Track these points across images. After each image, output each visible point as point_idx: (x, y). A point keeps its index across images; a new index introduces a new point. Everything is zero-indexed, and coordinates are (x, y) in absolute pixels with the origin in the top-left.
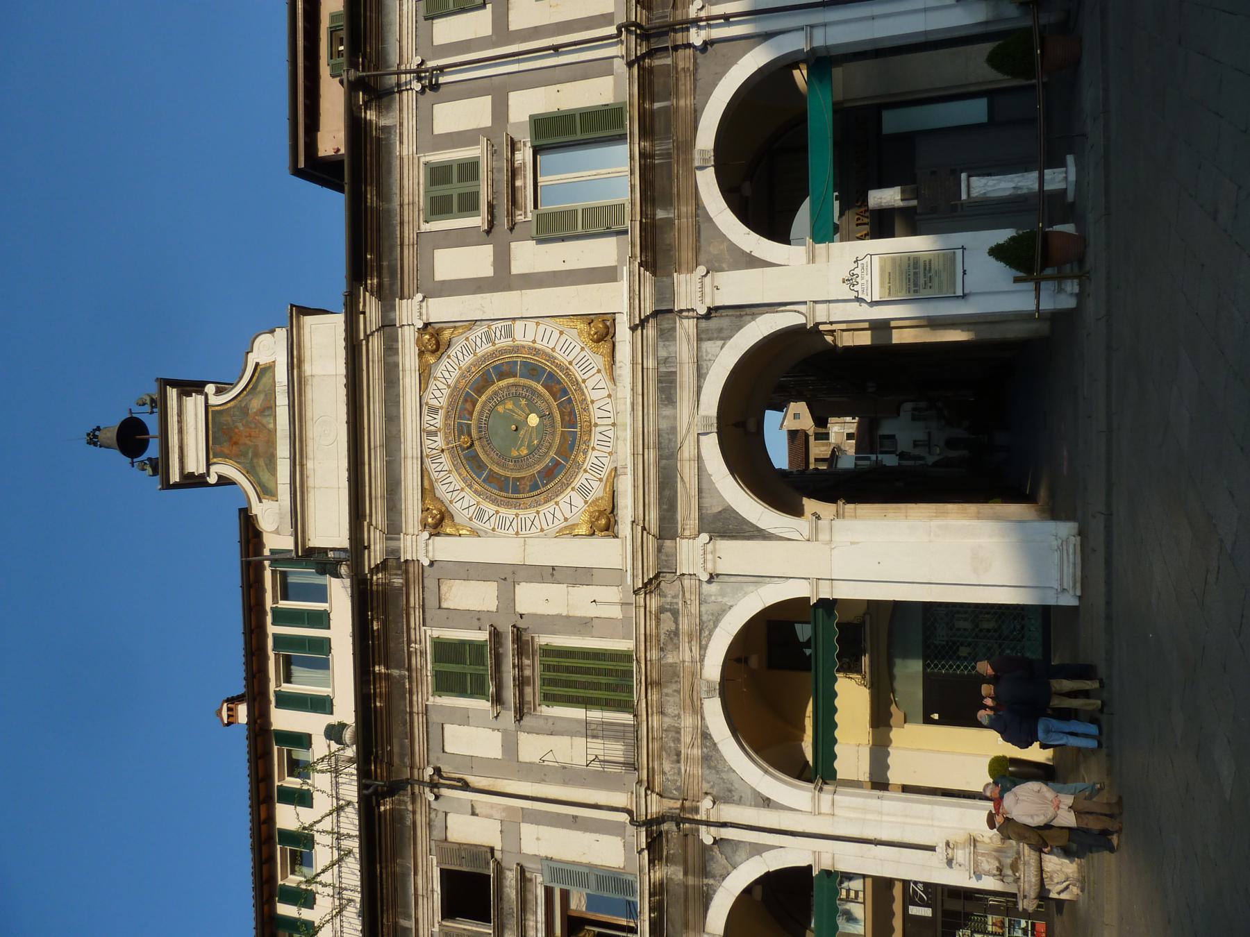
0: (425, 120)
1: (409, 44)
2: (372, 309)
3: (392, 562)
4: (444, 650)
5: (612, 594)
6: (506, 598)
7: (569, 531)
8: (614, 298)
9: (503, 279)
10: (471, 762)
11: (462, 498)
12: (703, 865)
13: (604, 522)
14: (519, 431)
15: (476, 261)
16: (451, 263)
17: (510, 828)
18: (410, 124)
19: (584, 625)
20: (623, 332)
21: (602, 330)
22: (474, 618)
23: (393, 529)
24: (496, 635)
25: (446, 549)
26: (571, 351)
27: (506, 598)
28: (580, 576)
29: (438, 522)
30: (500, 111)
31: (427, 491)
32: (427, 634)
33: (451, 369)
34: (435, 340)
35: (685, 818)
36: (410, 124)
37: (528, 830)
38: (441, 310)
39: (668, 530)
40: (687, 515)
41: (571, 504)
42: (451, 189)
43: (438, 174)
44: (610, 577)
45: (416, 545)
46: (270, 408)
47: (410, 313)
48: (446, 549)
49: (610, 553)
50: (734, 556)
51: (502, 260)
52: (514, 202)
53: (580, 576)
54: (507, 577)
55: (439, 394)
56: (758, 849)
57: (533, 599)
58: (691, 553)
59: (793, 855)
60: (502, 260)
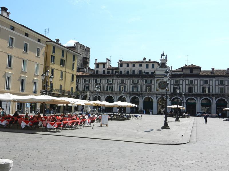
0: (181, 80)
1: (186, 79)
5: (153, 91)
7: (157, 88)
10: (143, 82)
11: (159, 82)
12: (139, 96)
13: (157, 90)
15: (172, 83)
16: (172, 81)
17: (140, 84)
18: (181, 79)
23: (157, 77)
25: (156, 81)
28: (154, 89)
29: (157, 80)
30: (181, 85)
31: (159, 79)
35: (142, 95)
36: (181, 79)
37: (140, 85)
39: (157, 94)
40: (157, 95)
41: (158, 88)
42: (177, 82)
43: (178, 81)
44: (154, 91)
45: (156, 79)
46: (165, 68)
48: (156, 81)
49: (155, 91)
50: (155, 98)
51: (172, 85)
53: (154, 89)
54: (154, 85)
56: (140, 98)
58: (155, 95)
59: (140, 100)
60: (172, 85)
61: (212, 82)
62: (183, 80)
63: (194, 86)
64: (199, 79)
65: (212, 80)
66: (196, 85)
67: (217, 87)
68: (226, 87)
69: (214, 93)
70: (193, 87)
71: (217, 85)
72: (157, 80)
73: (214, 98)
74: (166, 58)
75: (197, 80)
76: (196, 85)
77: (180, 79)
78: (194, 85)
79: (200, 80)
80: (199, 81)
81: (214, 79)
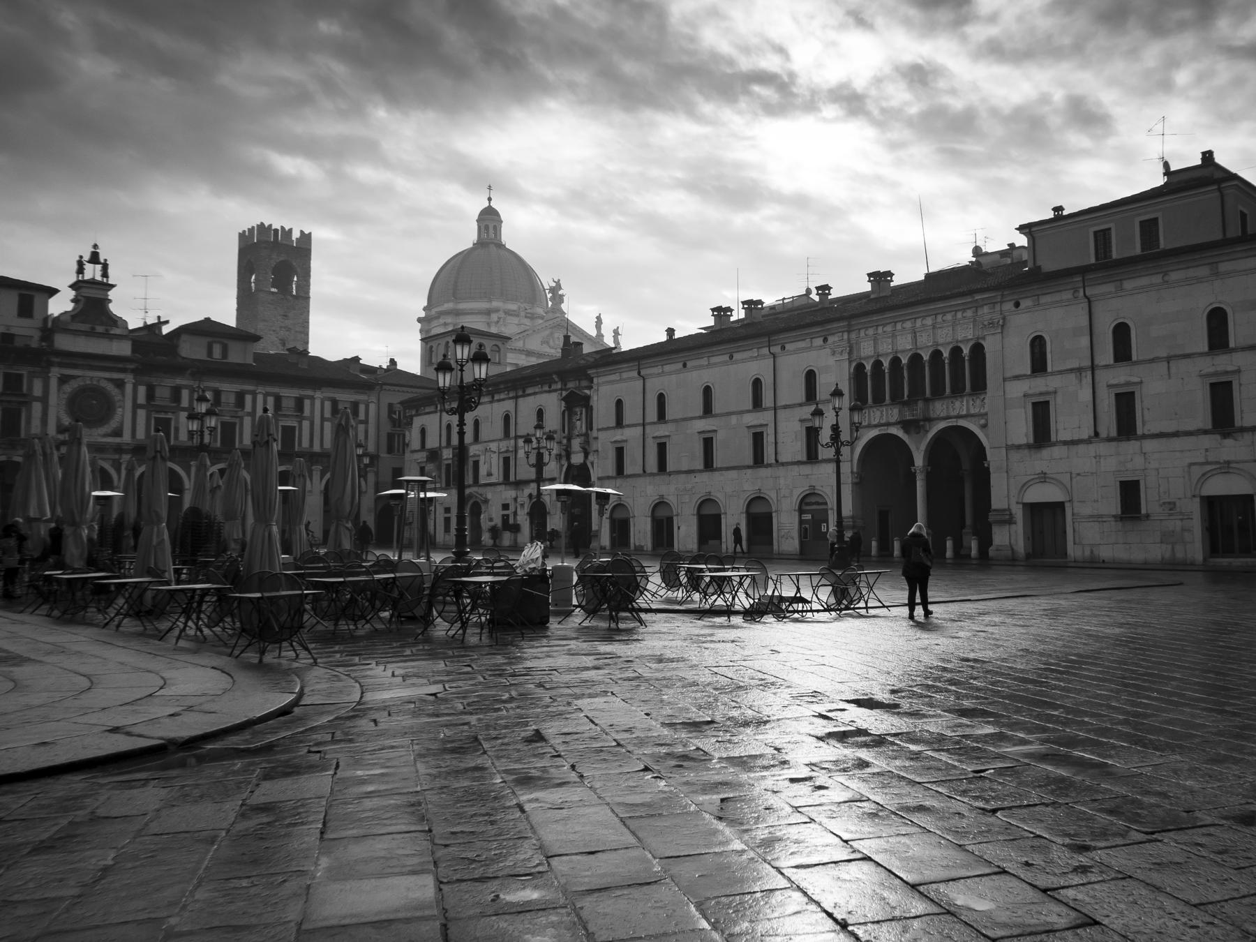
2: (132, 366)
3: (50, 364)
4: (20, 377)
6: (37, 399)
8: (127, 437)
9: (136, 406)
14: (90, 407)
18: (184, 382)
19: (29, 422)
20: (118, 440)
21: (118, 433)
22: (30, 388)
23: (61, 365)
24: (24, 395)
25: (54, 383)
26: (113, 424)
27: (37, 399)
28: (44, 421)
29: (63, 380)
32: (24, 371)
33: (110, 387)
34: (120, 384)
36: (184, 382)
38: (129, 388)
45: (55, 372)
46: (102, 324)
47: (129, 379)
48: (54, 383)
52: (158, 412)
54: (44, 400)
55: (104, 384)
57: (37, 407)
61: (313, 405)
62: (192, 391)
63: (241, 418)
64: (260, 389)
65: (312, 398)
66: (248, 414)
67: (327, 425)
68: (361, 427)
69: (317, 448)
70: (237, 421)
71: (328, 420)
72: (63, 380)
73: (317, 469)
74: (105, 274)
75: (254, 394)
76: (248, 414)
77: (179, 381)
78: (240, 414)
79: (266, 395)
80: (260, 398)
81: (318, 395)
